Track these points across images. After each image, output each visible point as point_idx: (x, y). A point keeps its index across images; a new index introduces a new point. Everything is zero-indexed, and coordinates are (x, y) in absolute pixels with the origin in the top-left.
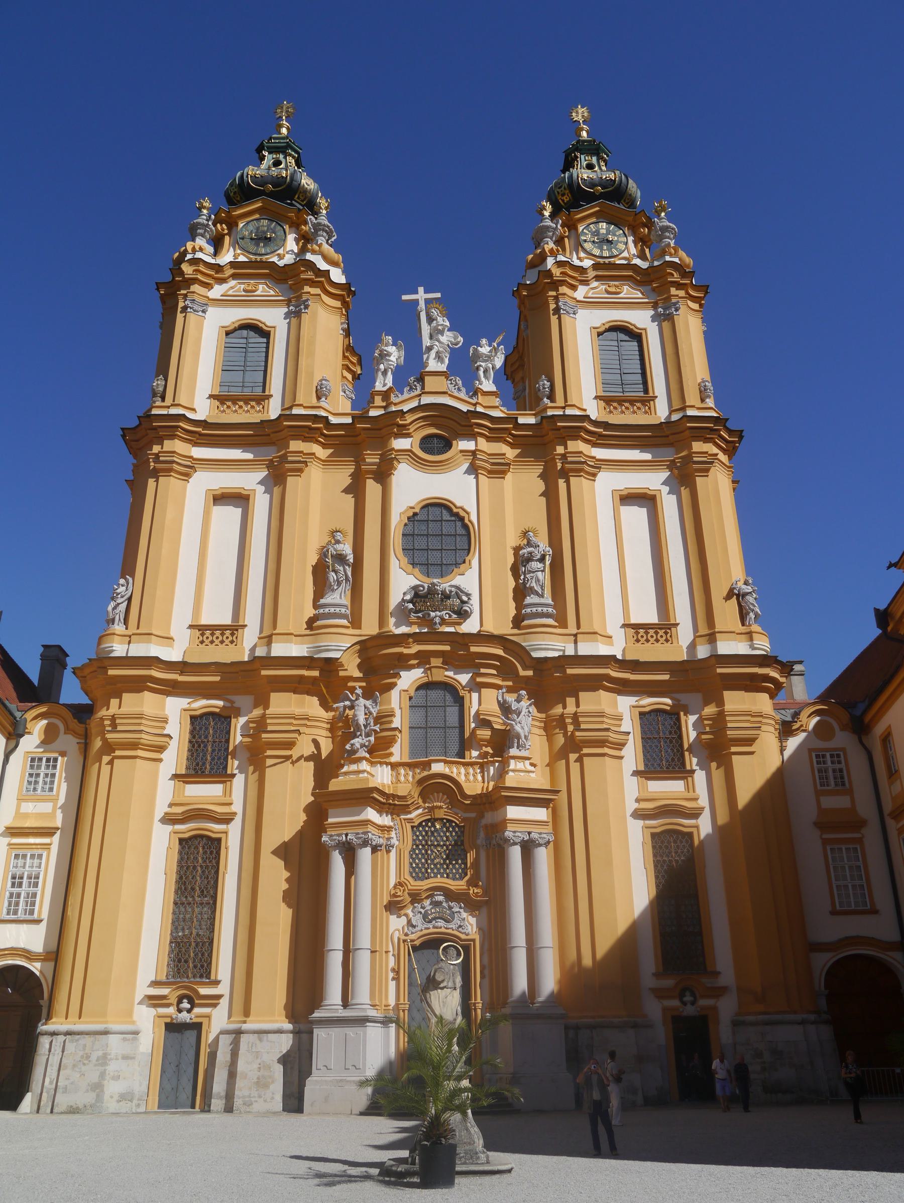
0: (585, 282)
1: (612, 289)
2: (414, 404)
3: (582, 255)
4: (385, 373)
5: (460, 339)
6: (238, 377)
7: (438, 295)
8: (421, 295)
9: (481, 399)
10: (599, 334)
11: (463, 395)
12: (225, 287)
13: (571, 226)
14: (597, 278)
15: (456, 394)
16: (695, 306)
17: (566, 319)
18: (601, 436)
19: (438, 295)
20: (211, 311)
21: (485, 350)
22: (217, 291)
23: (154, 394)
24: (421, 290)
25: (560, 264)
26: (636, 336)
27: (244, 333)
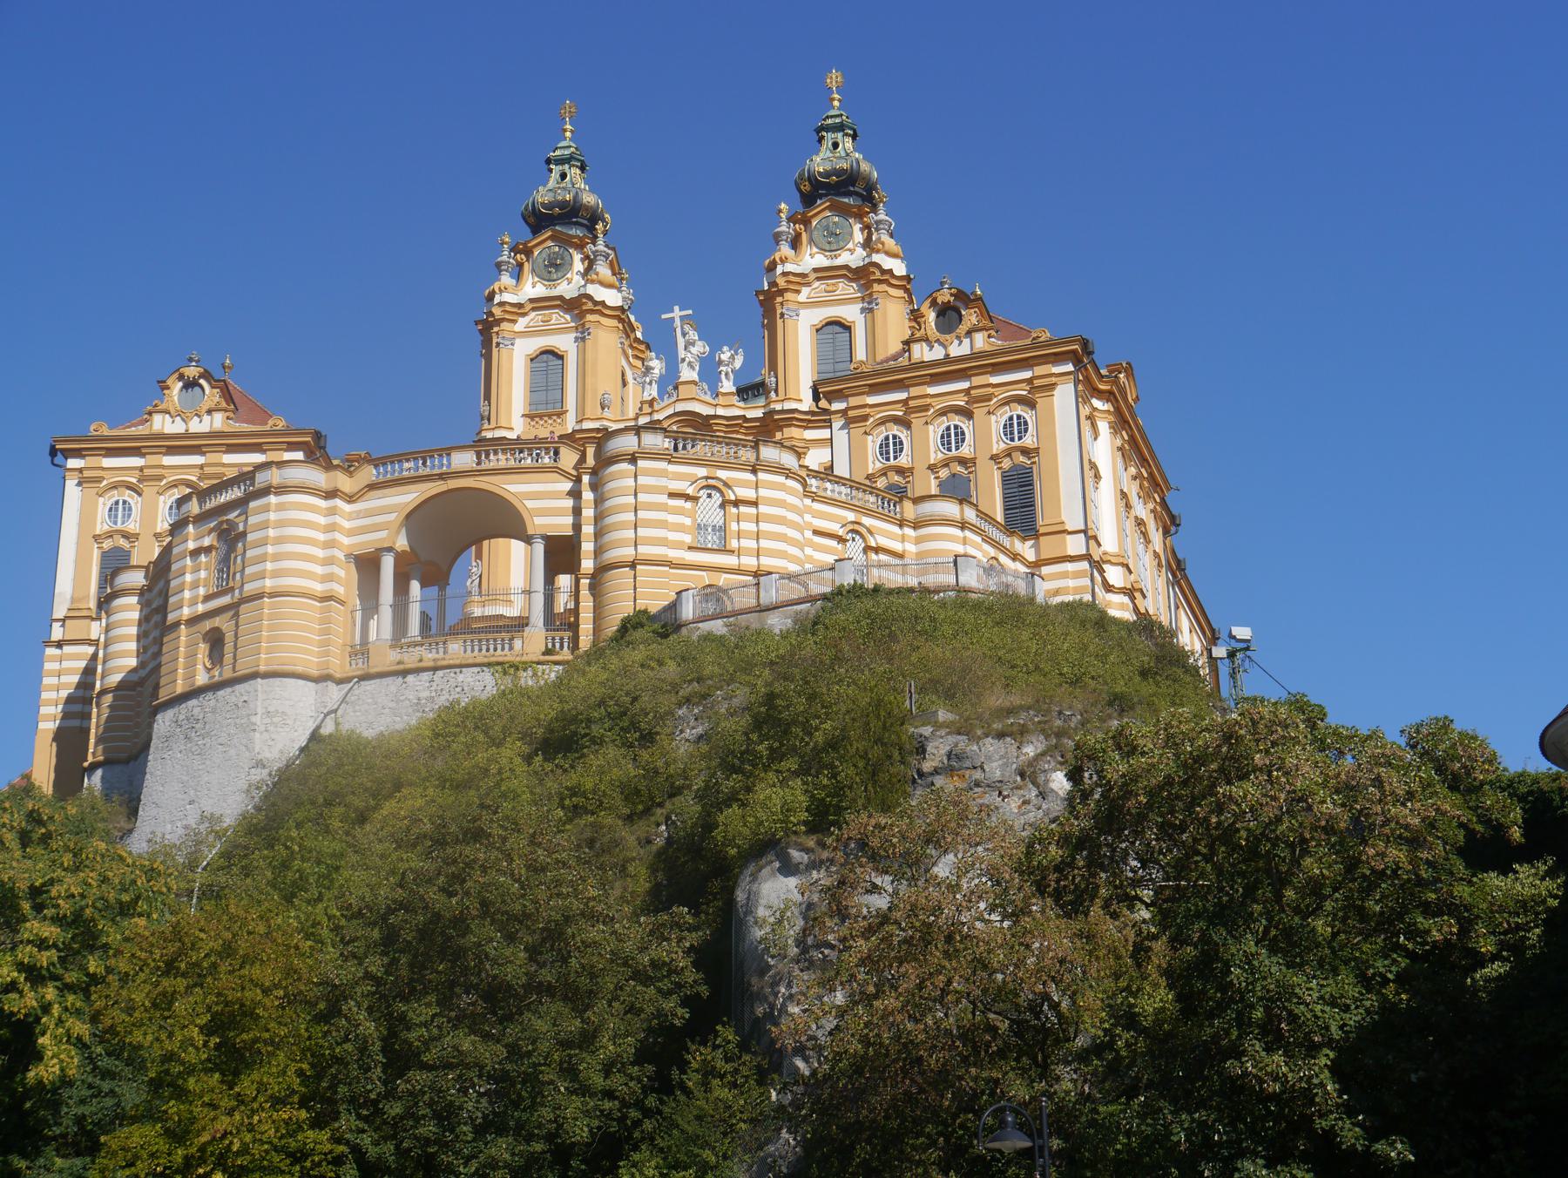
0: (808, 284)
1: (830, 288)
2: (670, 411)
3: (815, 250)
4: (650, 383)
5: (707, 348)
6: (542, 396)
7: (690, 312)
8: (677, 313)
9: (721, 400)
10: (817, 331)
11: (708, 398)
12: (527, 319)
13: (806, 222)
14: (818, 279)
15: (703, 397)
16: (900, 293)
17: (789, 322)
18: (810, 421)
19: (690, 312)
20: (518, 341)
21: (725, 357)
22: (521, 324)
23: (482, 419)
24: (676, 308)
25: (785, 274)
26: (847, 328)
27: (545, 357)
